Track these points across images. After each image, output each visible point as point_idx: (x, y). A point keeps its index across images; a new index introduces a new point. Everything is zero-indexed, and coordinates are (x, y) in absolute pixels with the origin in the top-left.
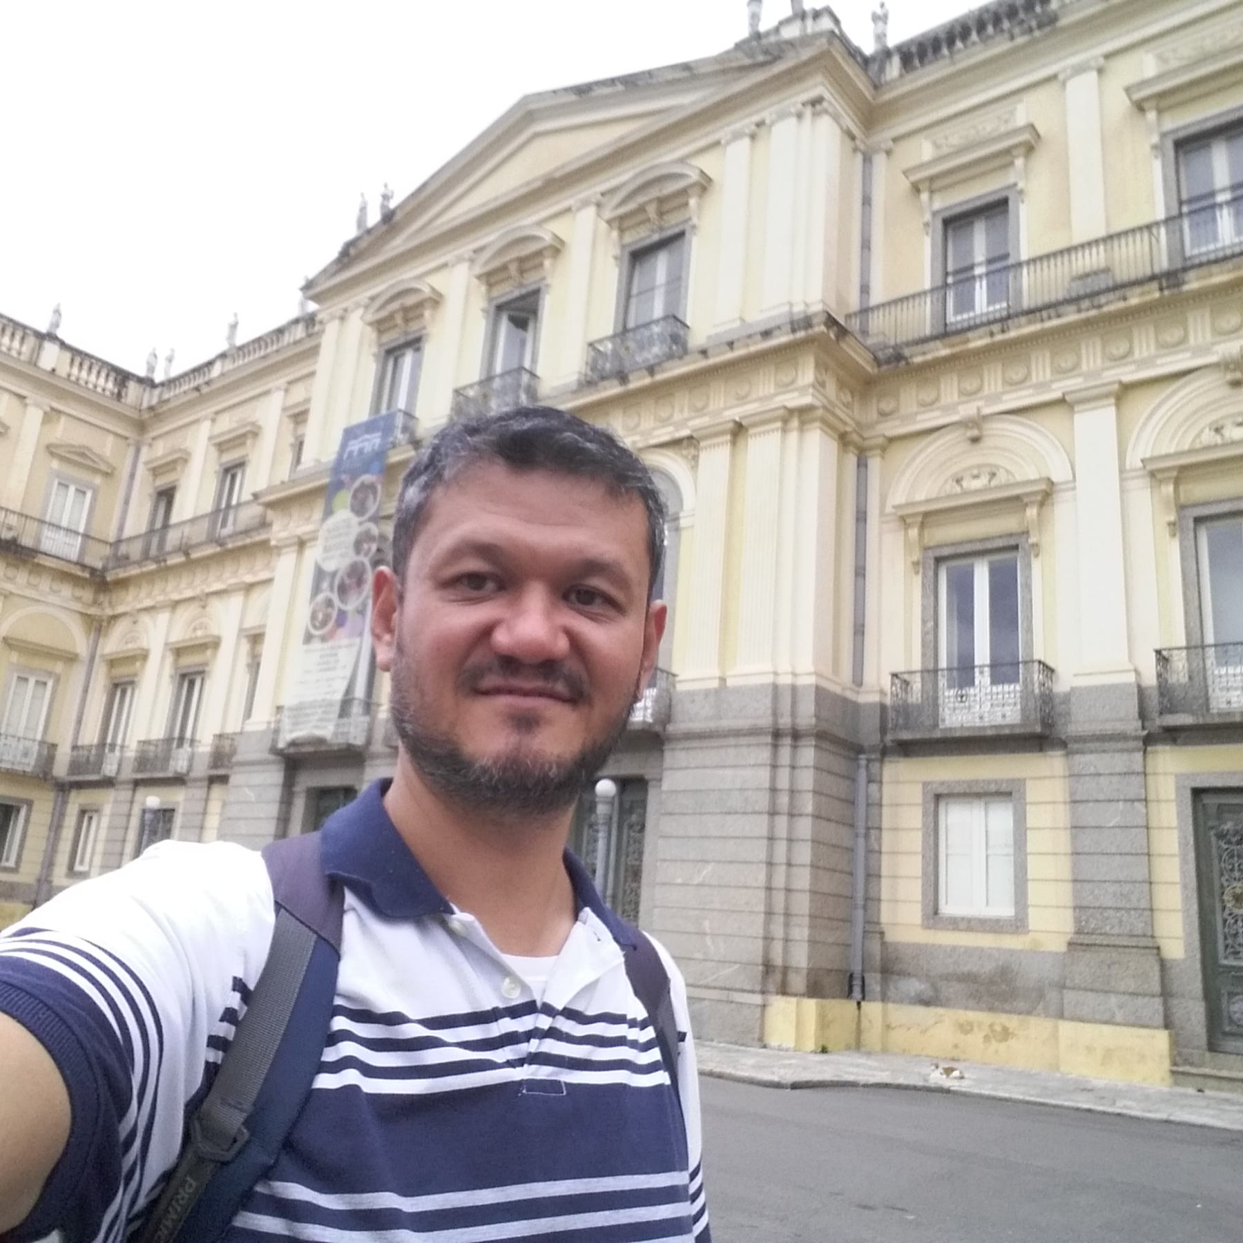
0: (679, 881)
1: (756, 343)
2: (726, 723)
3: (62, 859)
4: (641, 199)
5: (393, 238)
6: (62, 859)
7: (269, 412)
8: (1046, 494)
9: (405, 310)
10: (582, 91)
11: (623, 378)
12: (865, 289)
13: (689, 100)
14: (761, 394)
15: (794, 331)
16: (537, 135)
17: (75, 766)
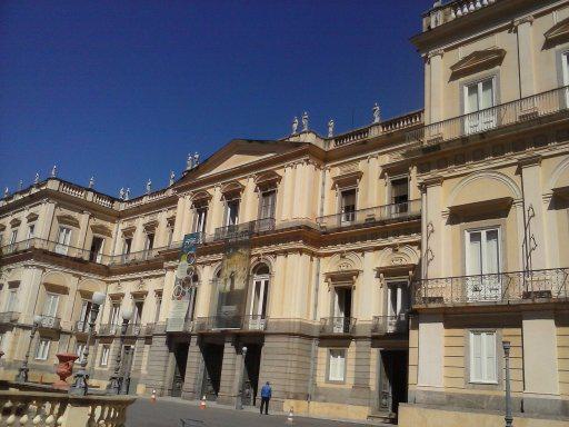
3: (97, 361)
6: (97, 361)
7: (162, 217)
8: (357, 273)
12: (322, 210)
17: (101, 330)
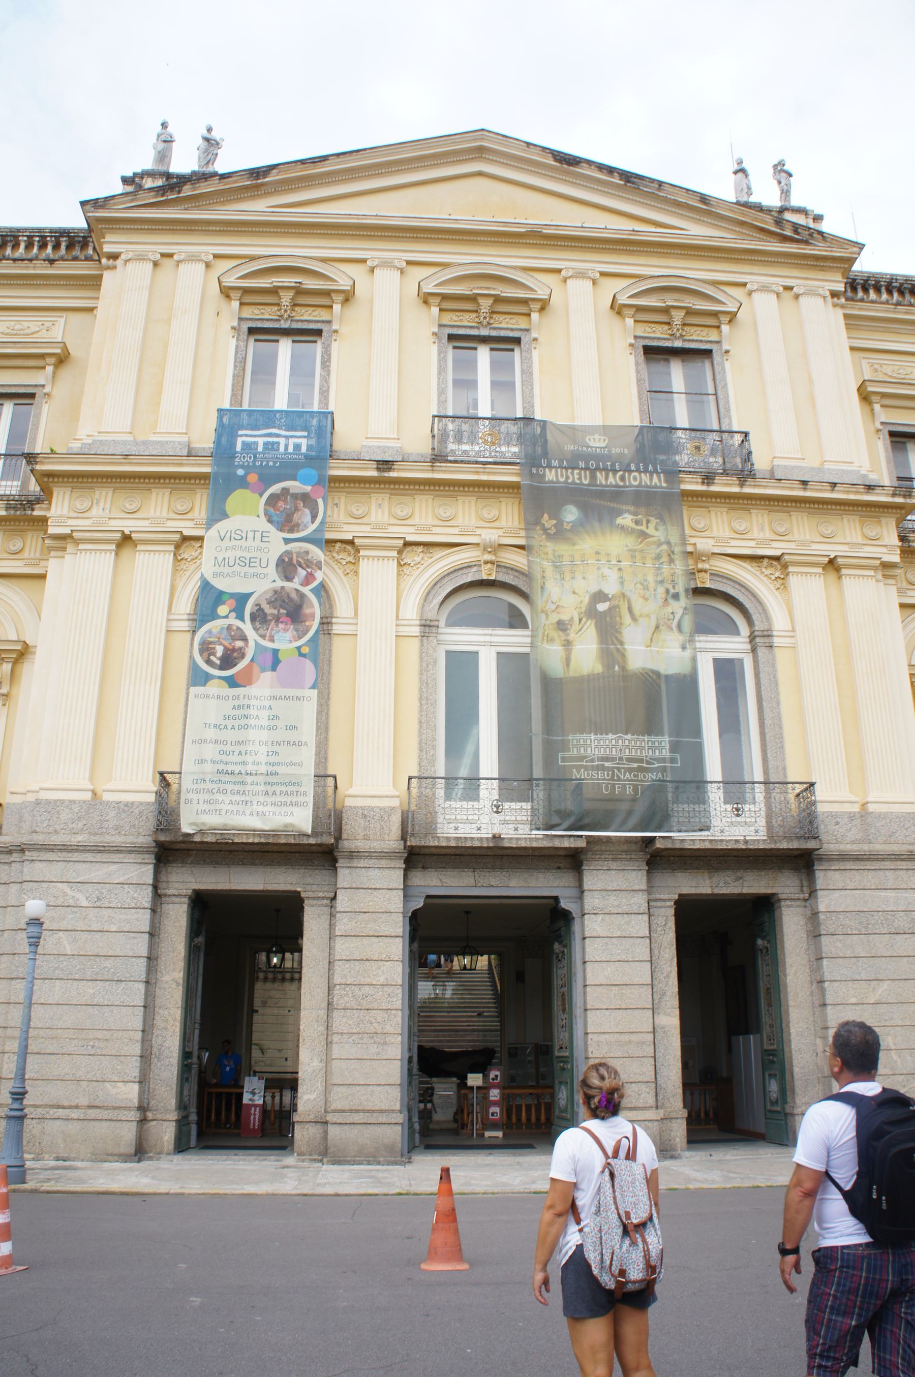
0: (853, 1000)
1: (857, 493)
2: (878, 847)
4: (671, 300)
5: (253, 198)
9: (299, 291)
10: (568, 161)
11: (708, 478)
13: (697, 231)
14: (848, 540)
15: (894, 495)
16: (480, 174)
